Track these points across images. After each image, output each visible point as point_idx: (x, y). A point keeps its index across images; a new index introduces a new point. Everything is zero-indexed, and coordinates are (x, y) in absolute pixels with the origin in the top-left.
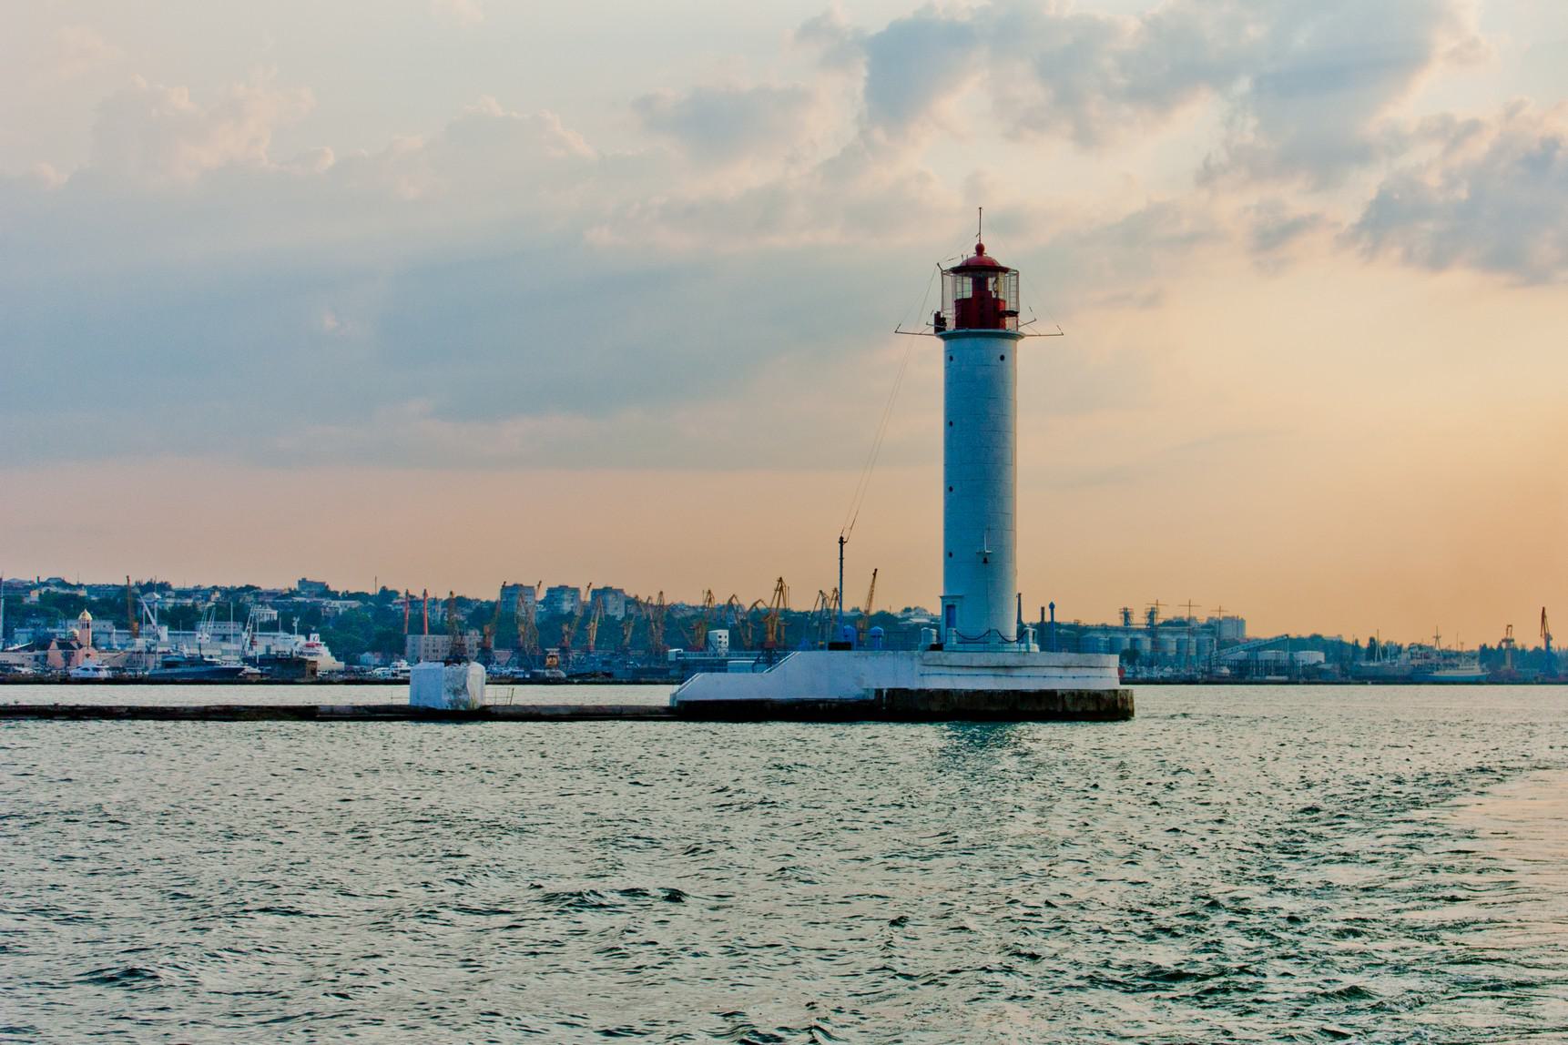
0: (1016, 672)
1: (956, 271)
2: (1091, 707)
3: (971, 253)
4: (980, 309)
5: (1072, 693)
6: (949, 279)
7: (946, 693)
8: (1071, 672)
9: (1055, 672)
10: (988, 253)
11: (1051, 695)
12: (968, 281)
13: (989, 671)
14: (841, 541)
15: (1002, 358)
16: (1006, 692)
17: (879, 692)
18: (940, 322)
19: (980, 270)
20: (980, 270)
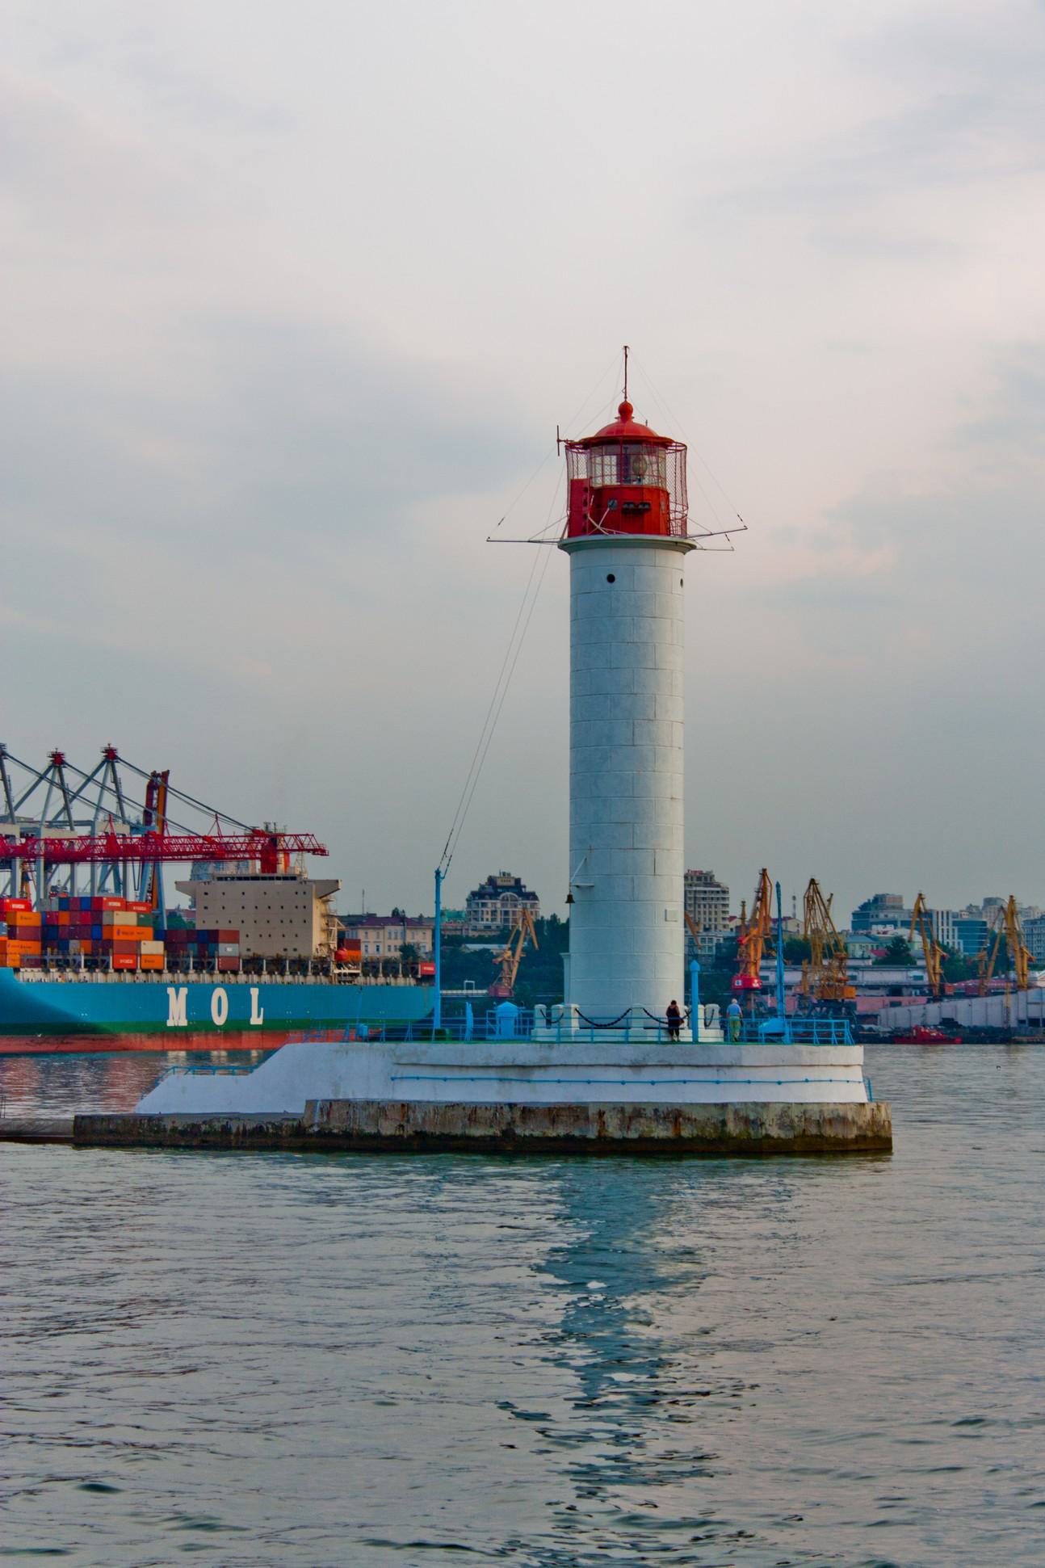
0: (537, 1075)
1: (588, 444)
2: (661, 1132)
3: (611, 417)
4: (622, 498)
5: (620, 1108)
6: (582, 459)
7: (405, 1107)
8: (647, 1074)
9: (613, 1074)
10: (637, 418)
11: (577, 1112)
12: (611, 461)
13: (492, 1073)
14: (438, 873)
15: (611, 579)
16: (498, 1107)
17: (310, 1104)
18: (576, 525)
19: (627, 440)
20: (627, 440)
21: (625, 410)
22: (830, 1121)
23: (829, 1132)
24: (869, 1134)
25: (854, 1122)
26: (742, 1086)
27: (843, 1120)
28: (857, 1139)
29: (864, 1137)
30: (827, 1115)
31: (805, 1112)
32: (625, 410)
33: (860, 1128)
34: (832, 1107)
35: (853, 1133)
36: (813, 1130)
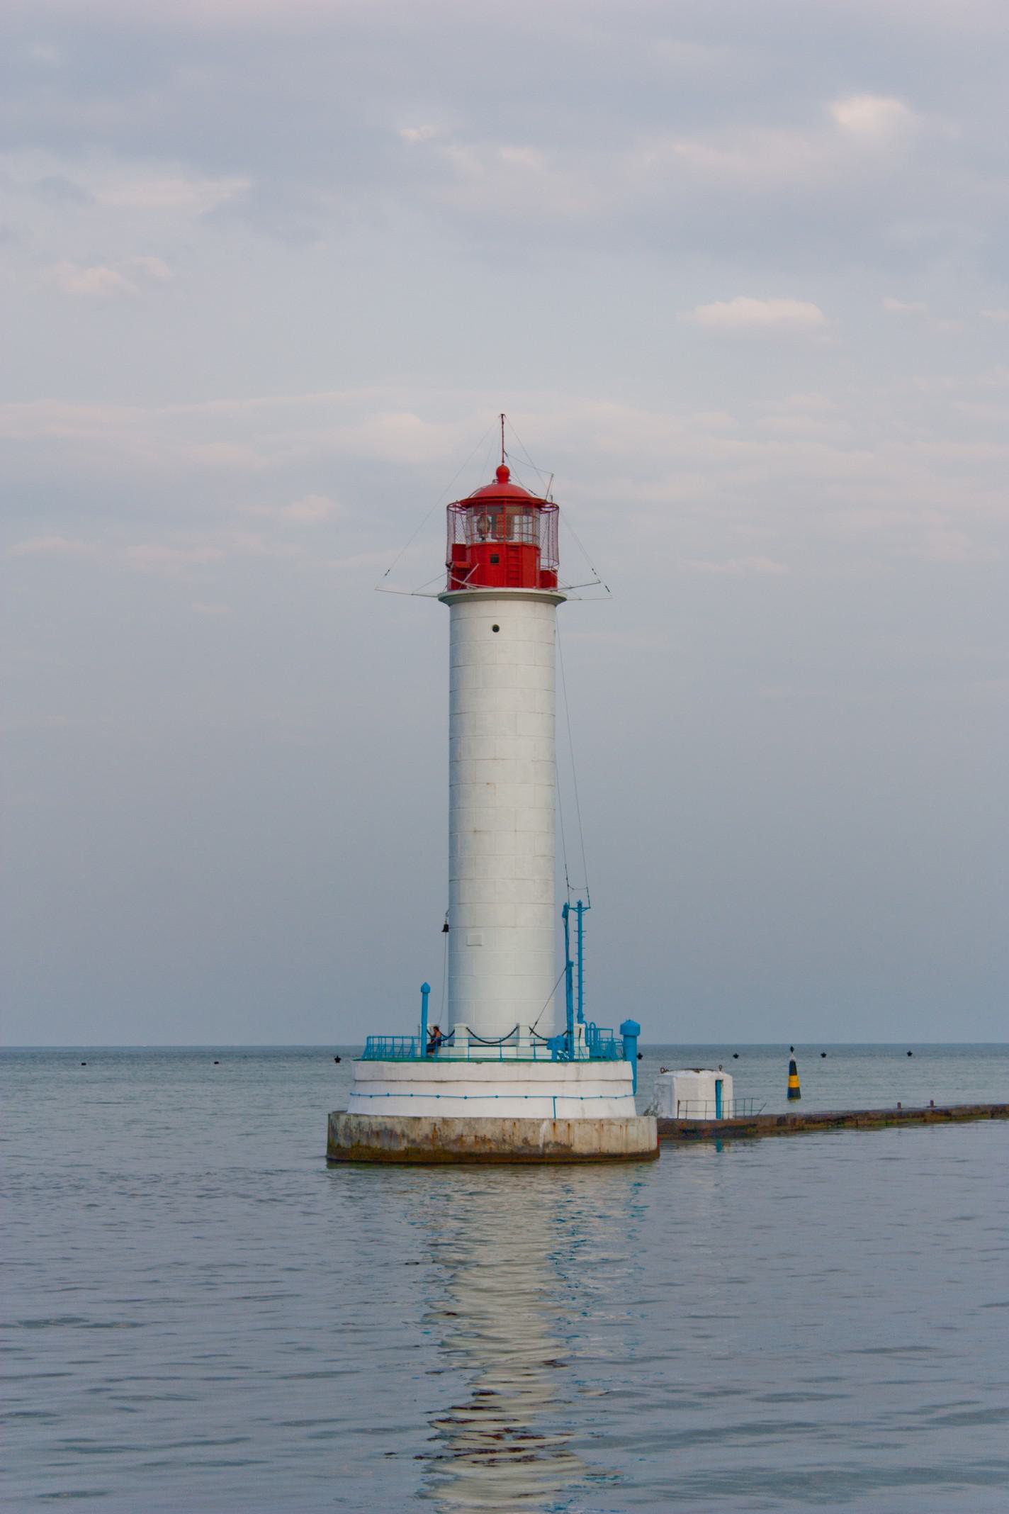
19: (499, 501)
20: (499, 501)
21: (503, 474)
22: (378, 1134)
23: (376, 1144)
24: (427, 1147)
25: (403, 1135)
26: (519, 1100)
27: (391, 1134)
28: (407, 1152)
29: (418, 1151)
30: (375, 1128)
31: (359, 1124)
32: (503, 474)
33: (413, 1141)
34: (380, 1120)
35: (404, 1145)
36: (364, 1142)
